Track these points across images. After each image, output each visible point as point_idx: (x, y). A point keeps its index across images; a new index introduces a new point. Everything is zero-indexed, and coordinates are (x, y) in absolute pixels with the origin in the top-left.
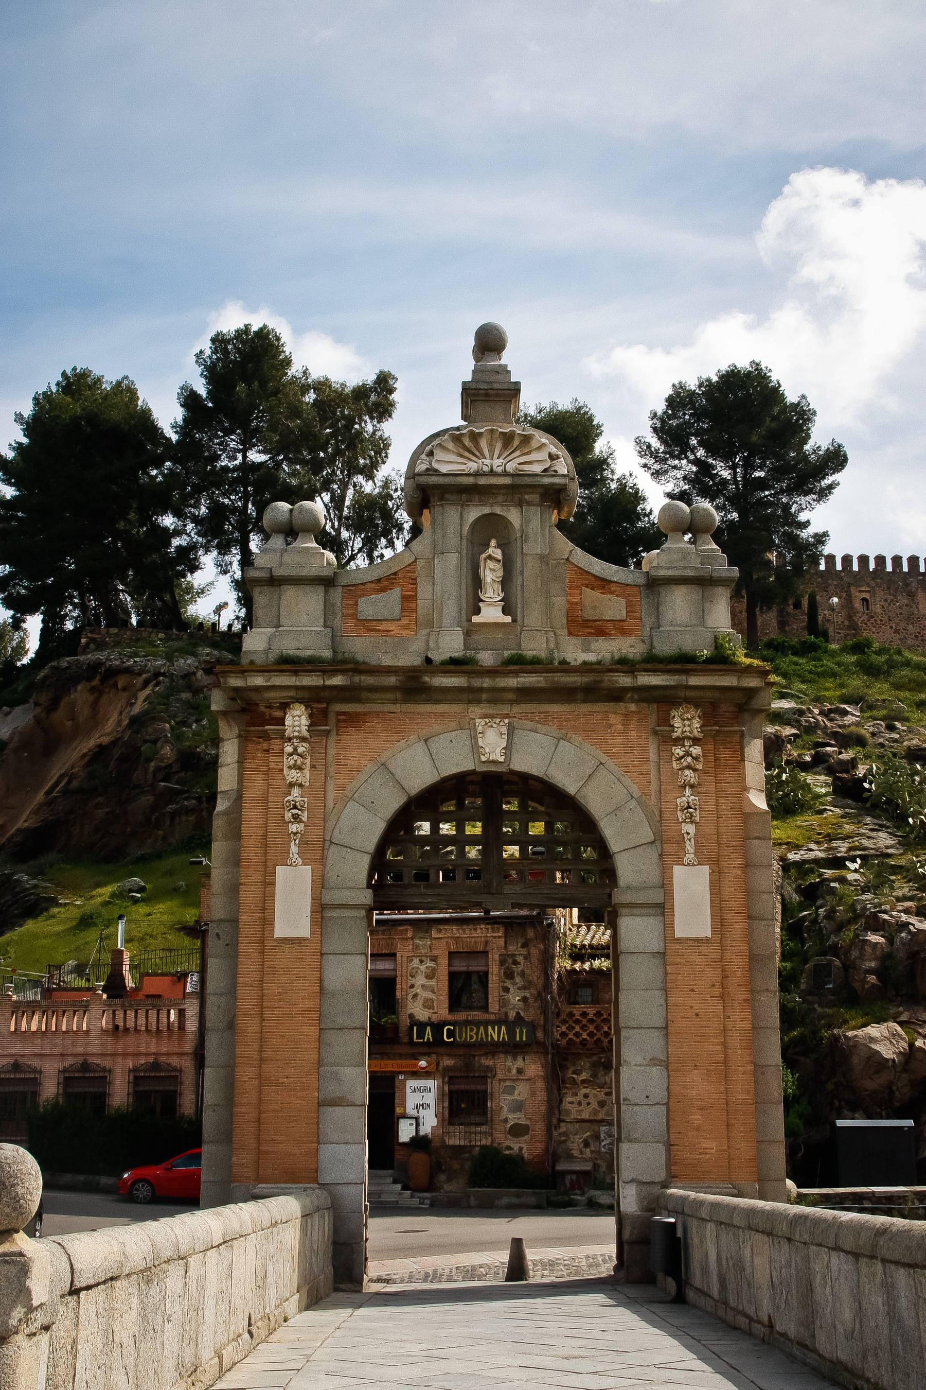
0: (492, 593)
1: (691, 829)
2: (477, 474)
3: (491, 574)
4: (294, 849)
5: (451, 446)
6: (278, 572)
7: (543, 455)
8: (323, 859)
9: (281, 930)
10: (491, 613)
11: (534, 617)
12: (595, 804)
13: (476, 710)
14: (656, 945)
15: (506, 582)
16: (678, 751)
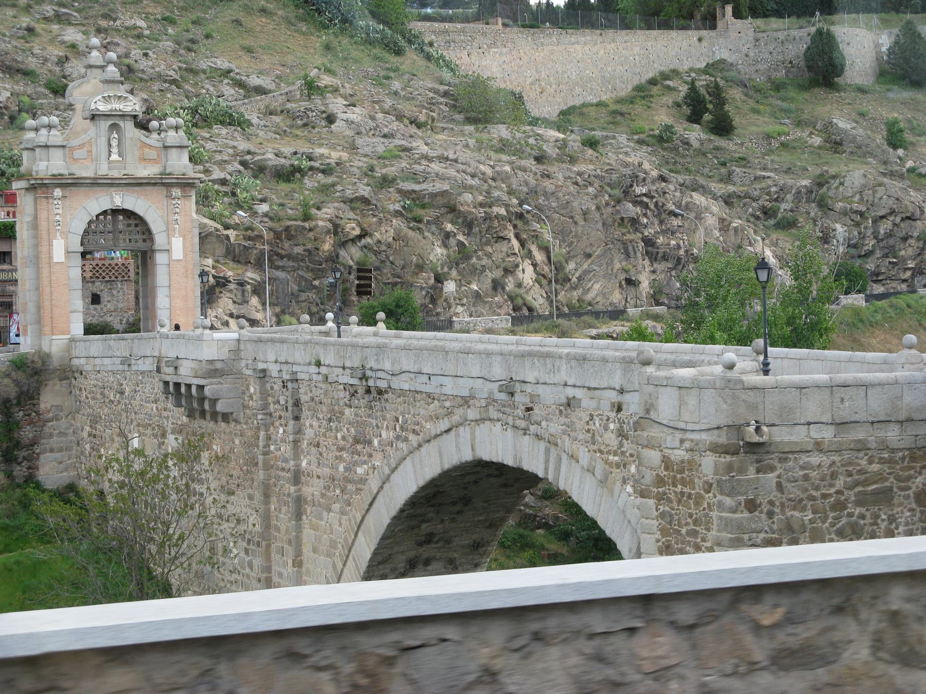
0: (115, 150)
1: (177, 226)
2: (111, 110)
3: (114, 143)
4: (58, 234)
5: (102, 100)
6: (49, 144)
7: (131, 104)
8: (67, 238)
9: (55, 260)
10: (115, 157)
11: (129, 159)
12: (149, 218)
13: (112, 189)
14: (167, 262)
15: (119, 145)
16: (174, 202)
